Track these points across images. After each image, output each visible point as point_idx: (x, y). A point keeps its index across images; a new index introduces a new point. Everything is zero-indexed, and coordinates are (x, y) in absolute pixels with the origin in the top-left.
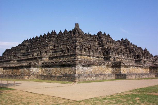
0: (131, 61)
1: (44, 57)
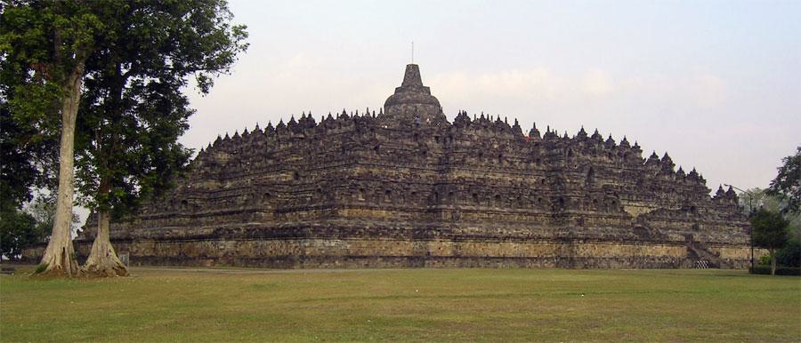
0: (533, 218)
1: (260, 211)
